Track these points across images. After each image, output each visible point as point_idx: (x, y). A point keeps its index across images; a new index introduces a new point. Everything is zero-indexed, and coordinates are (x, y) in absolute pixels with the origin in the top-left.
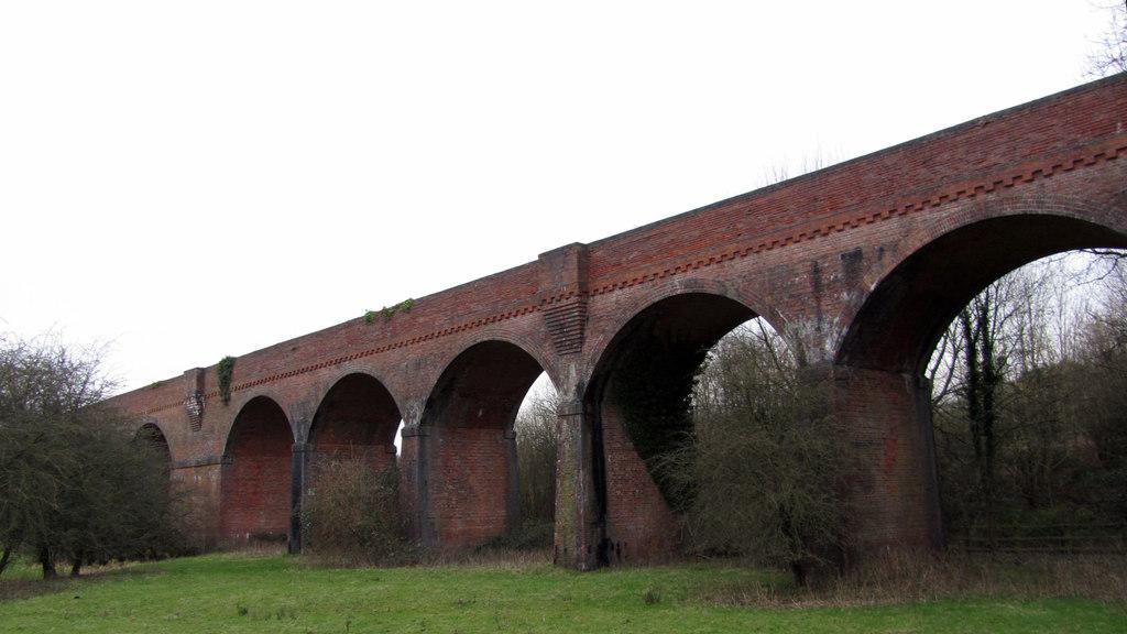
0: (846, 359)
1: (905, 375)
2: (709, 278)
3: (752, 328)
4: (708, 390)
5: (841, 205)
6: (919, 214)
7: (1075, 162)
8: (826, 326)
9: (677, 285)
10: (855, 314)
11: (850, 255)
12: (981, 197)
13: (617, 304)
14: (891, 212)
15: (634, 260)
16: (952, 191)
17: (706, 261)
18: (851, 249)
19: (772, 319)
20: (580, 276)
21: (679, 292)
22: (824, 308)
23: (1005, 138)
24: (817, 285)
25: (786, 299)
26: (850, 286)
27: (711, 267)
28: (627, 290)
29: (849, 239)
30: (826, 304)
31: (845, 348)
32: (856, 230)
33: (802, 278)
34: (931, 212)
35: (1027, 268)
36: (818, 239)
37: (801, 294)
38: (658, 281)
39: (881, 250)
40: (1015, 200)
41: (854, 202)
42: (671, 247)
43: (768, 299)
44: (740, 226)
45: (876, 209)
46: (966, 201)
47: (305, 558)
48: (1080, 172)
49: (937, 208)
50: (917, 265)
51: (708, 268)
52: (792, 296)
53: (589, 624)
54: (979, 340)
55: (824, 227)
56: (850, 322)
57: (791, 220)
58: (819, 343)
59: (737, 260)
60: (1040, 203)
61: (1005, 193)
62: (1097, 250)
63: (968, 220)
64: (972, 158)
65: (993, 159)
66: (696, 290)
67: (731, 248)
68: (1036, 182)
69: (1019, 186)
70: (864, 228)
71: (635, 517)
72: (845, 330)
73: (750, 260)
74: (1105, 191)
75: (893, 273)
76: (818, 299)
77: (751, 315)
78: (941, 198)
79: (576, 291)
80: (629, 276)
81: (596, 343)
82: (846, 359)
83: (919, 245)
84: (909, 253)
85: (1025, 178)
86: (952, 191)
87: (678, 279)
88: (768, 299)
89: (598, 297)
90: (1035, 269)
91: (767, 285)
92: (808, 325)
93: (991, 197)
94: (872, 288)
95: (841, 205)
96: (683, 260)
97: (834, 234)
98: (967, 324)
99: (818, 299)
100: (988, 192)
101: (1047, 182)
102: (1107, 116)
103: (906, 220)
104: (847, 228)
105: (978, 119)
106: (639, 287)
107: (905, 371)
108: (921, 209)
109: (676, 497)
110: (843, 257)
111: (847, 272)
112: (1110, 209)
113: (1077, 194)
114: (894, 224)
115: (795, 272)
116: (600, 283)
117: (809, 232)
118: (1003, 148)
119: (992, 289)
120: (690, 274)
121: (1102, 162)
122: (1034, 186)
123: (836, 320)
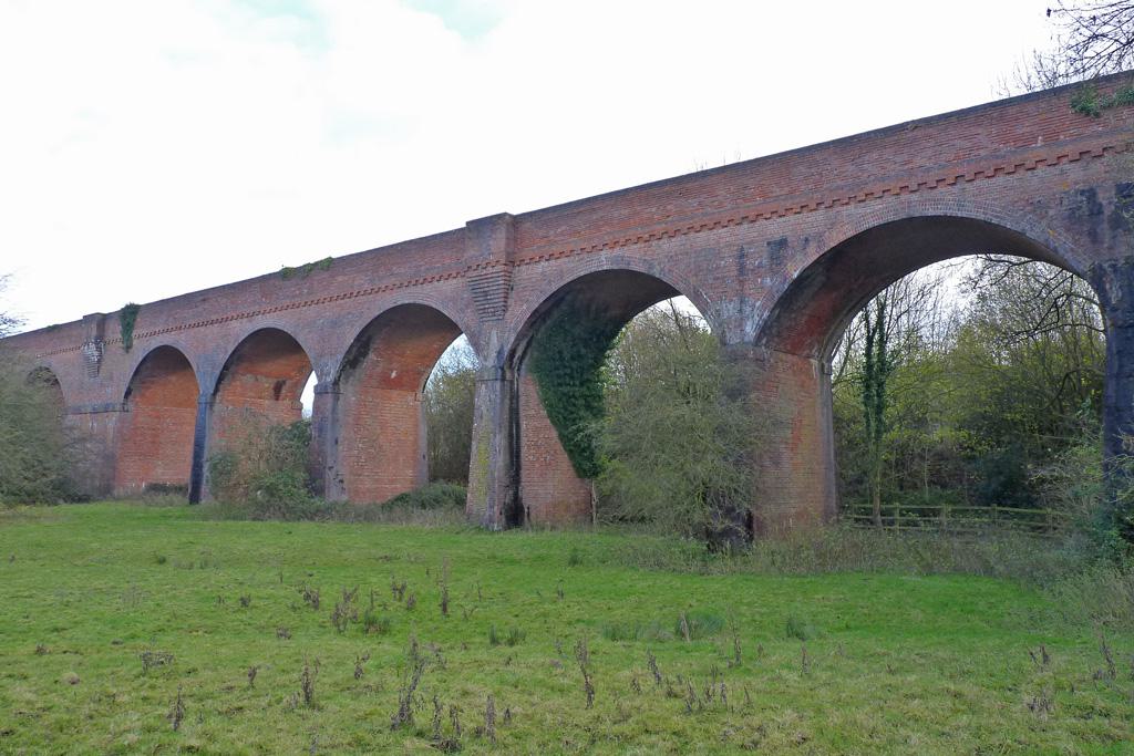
0: (764, 341)
1: (812, 360)
2: (635, 257)
3: (683, 304)
4: (615, 368)
5: (770, 195)
6: (845, 207)
7: (996, 170)
8: (748, 309)
9: (604, 261)
10: (776, 299)
11: (775, 243)
12: (904, 197)
13: (543, 277)
14: (818, 204)
15: (562, 234)
16: (877, 188)
17: (634, 239)
18: (777, 237)
19: (696, 299)
20: (508, 245)
21: (605, 268)
22: (747, 292)
23: (932, 143)
24: (742, 269)
25: (710, 282)
26: (774, 273)
27: (638, 245)
28: (552, 262)
29: (775, 228)
30: (749, 288)
31: (764, 330)
32: (783, 219)
33: (728, 262)
34: (855, 208)
35: (922, 271)
36: (745, 226)
37: (725, 277)
38: (585, 255)
39: (807, 240)
40: (936, 201)
41: (783, 193)
42: (601, 223)
43: (693, 280)
44: (669, 207)
45: (804, 201)
46: (890, 199)
47: (1099, 474)
48: (1001, 179)
49: (862, 204)
50: (836, 259)
51: (635, 246)
52: (716, 279)
53: (1076, 668)
54: (877, 334)
55: (752, 215)
56: (772, 306)
57: (721, 205)
58: (740, 325)
59: (665, 240)
60: (961, 206)
61: (927, 194)
62: (992, 256)
63: (891, 218)
64: (898, 159)
65: (918, 161)
66: (623, 267)
67: (659, 228)
68: (958, 186)
69: (942, 189)
70: (791, 218)
71: (549, 481)
72: (766, 314)
73: (677, 241)
74: (1021, 199)
75: (817, 262)
76: (741, 283)
77: (670, 292)
78: (866, 195)
79: (503, 261)
80: (555, 249)
81: (520, 312)
82: (764, 341)
83: (843, 238)
84: (833, 245)
85: (948, 182)
86: (877, 188)
87: (604, 254)
88: (693, 280)
89: (523, 268)
90: (923, 275)
91: (692, 266)
92: (731, 307)
93: (915, 197)
94: (795, 275)
95: (770, 195)
96: (611, 237)
97: (761, 222)
98: (866, 318)
99: (741, 283)
100: (912, 192)
101: (967, 185)
102: (1029, 129)
103: (831, 212)
104: (775, 217)
105: (907, 123)
106: (566, 260)
107: (813, 356)
108: (847, 204)
109: (584, 460)
110: (769, 244)
111: (772, 259)
112: (1025, 216)
113: (994, 199)
114: (820, 216)
115: (722, 255)
116: (527, 254)
117: (737, 218)
118: (930, 152)
119: (891, 288)
120: (617, 251)
121: (1021, 171)
122: (955, 189)
123: (758, 304)
